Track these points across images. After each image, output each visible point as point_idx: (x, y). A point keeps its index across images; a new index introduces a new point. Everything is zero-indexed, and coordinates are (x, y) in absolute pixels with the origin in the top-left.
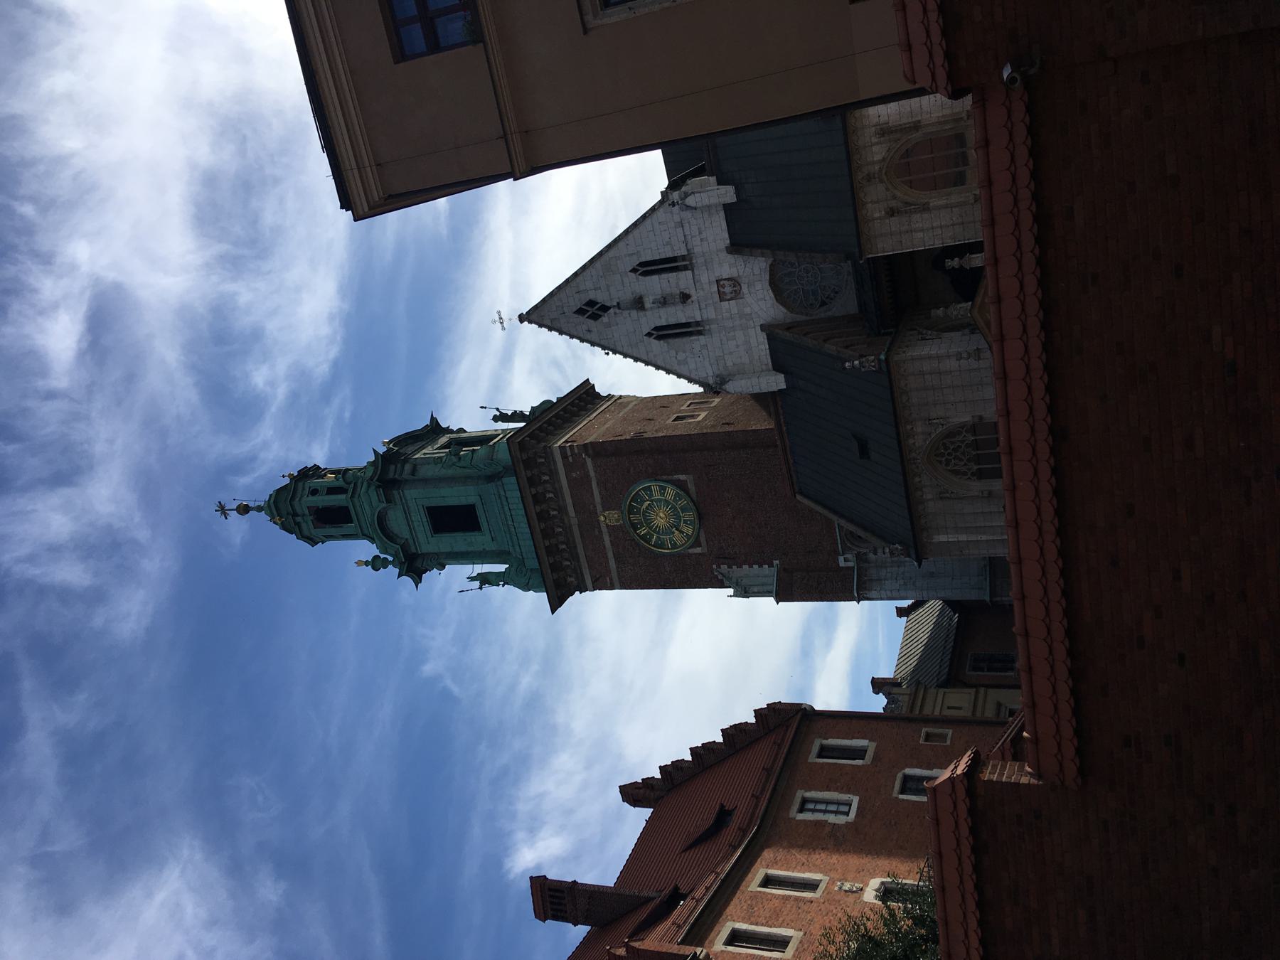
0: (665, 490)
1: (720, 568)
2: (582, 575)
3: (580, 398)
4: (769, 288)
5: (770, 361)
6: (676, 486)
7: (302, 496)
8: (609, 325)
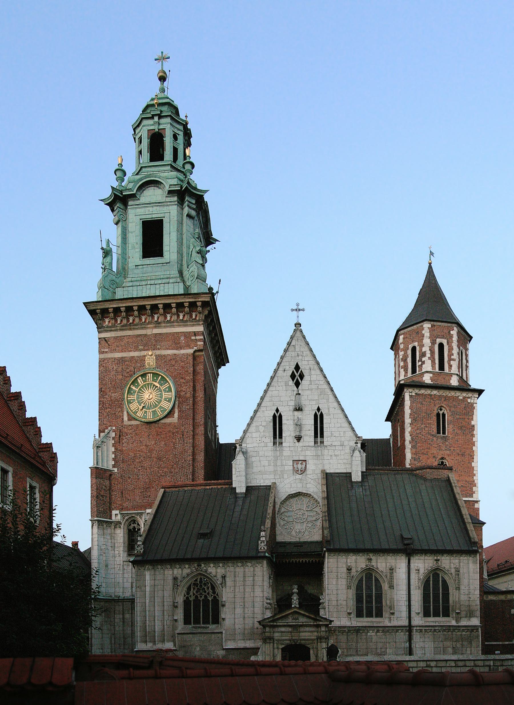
5: (253, 485)
6: (171, 409)
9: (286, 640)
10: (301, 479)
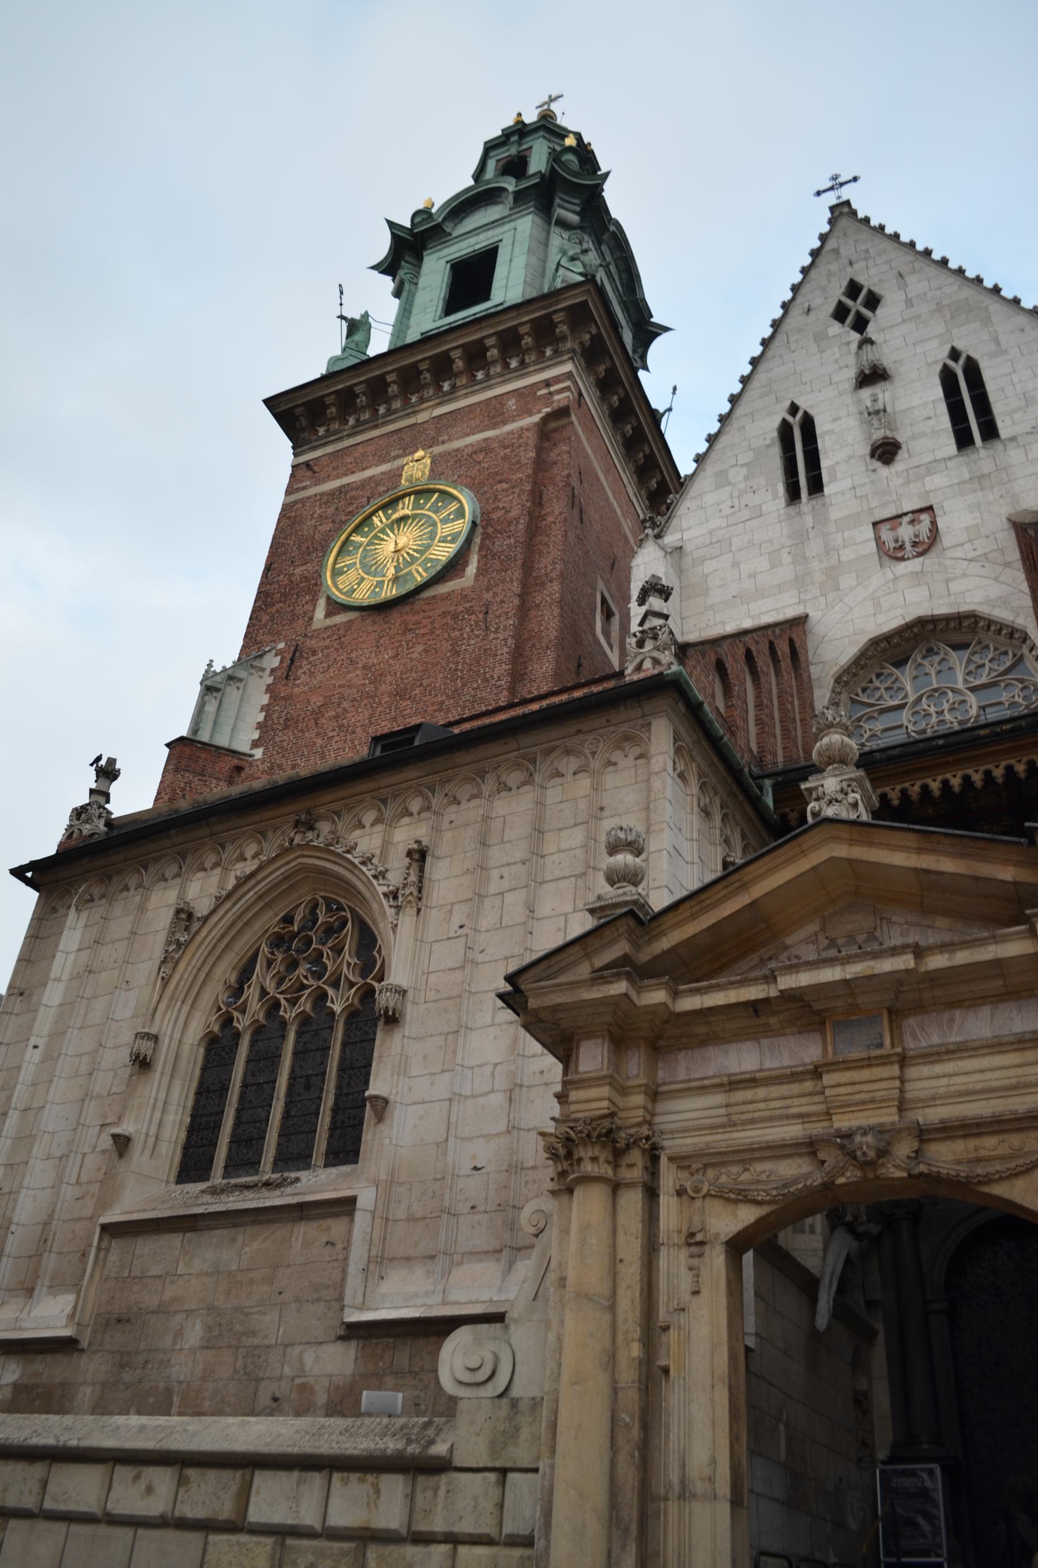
0: (453, 541)
1: (276, 655)
4: (909, 618)
7: (549, 141)
8: (820, 337)
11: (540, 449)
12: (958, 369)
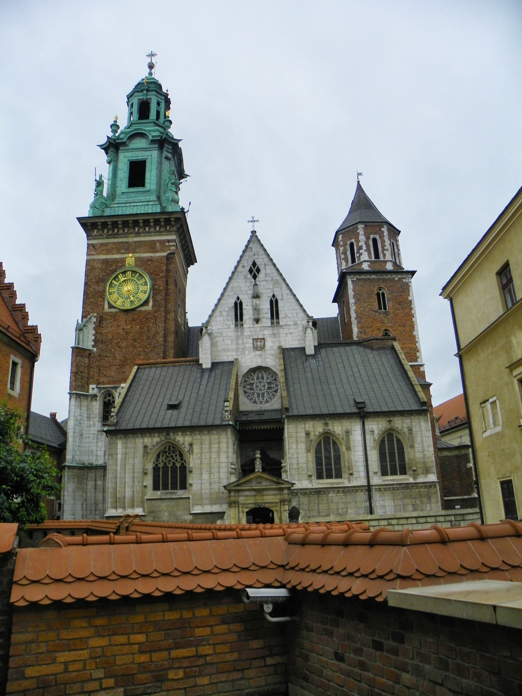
2: (98, 239)
3: (190, 256)
4: (258, 365)
7: (157, 97)
8: (246, 277)
9: (251, 504)
10: (260, 355)
11: (167, 264)
12: (274, 300)
